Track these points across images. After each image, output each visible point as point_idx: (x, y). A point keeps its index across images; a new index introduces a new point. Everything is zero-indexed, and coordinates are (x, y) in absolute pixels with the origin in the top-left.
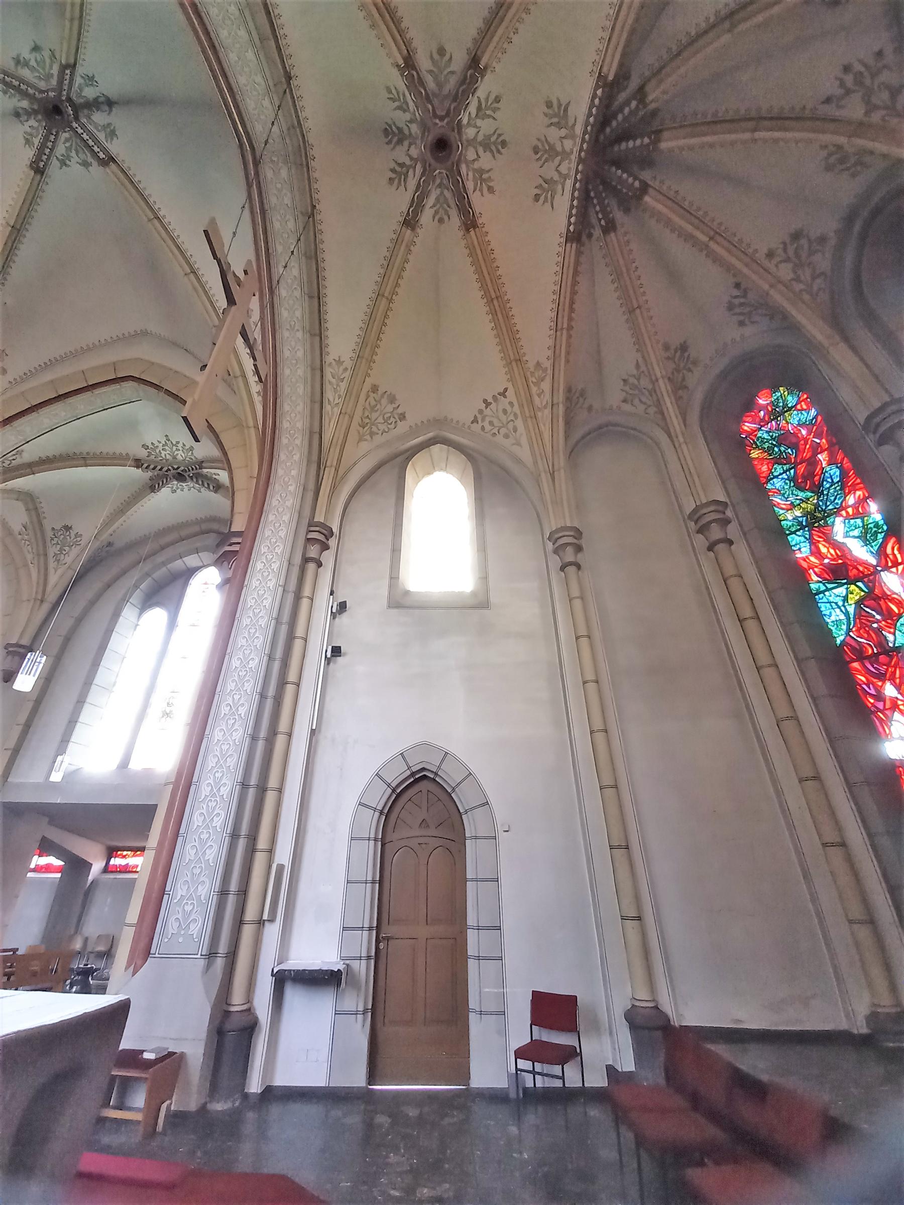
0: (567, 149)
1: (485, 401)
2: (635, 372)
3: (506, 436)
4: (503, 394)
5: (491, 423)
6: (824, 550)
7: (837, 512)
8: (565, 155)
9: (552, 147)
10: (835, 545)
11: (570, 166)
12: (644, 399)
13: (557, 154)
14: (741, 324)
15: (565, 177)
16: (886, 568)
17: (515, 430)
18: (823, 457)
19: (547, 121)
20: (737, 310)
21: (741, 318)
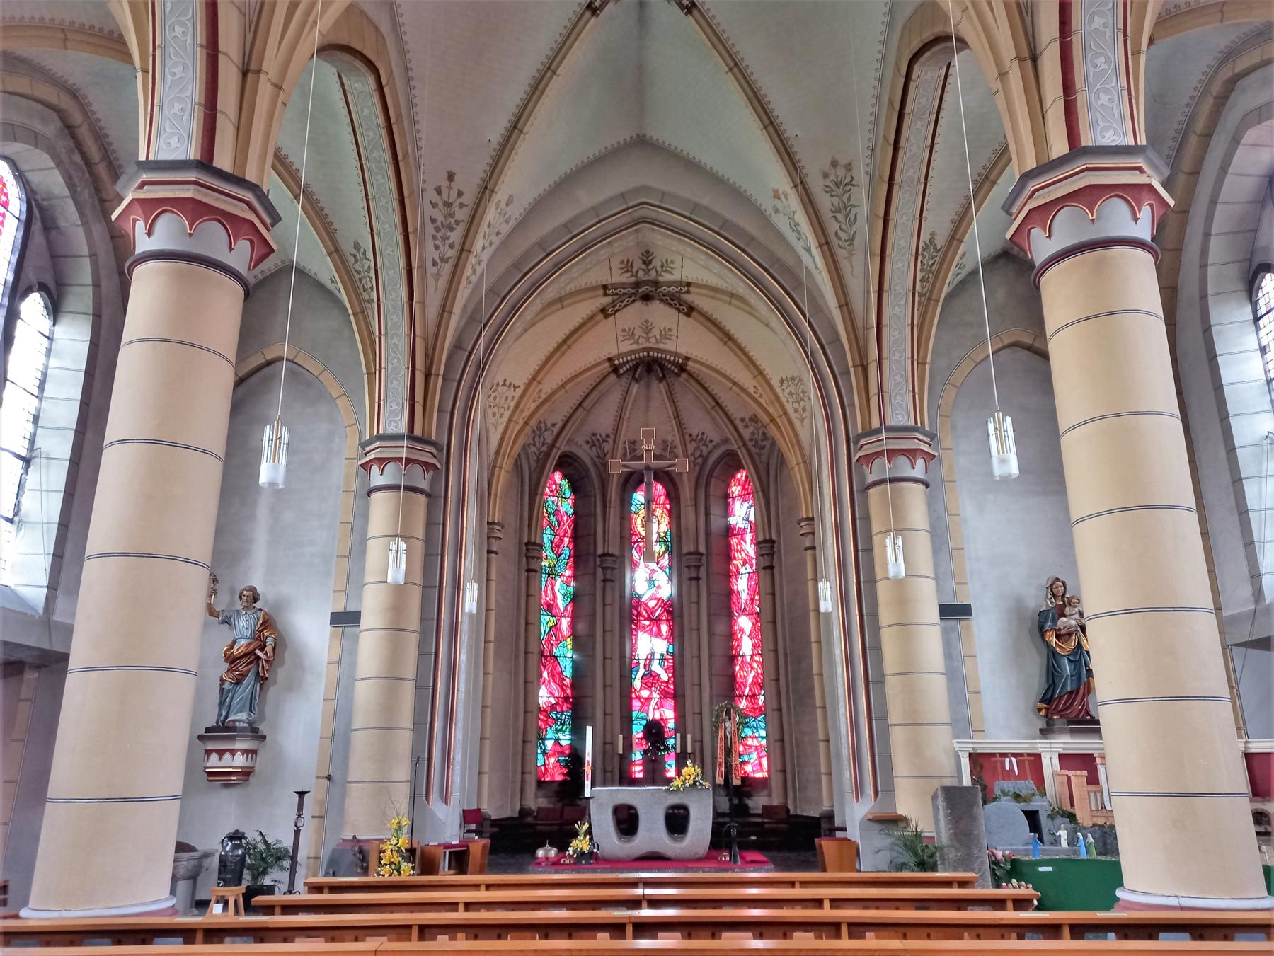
0: (651, 340)
1: (505, 380)
3: (494, 415)
4: (515, 387)
5: (495, 398)
6: (549, 592)
7: (560, 576)
8: (648, 339)
10: (554, 593)
12: (537, 438)
13: (647, 334)
14: (587, 442)
15: (637, 342)
16: (565, 616)
18: (566, 540)
19: (662, 329)
20: (594, 438)
21: (590, 440)
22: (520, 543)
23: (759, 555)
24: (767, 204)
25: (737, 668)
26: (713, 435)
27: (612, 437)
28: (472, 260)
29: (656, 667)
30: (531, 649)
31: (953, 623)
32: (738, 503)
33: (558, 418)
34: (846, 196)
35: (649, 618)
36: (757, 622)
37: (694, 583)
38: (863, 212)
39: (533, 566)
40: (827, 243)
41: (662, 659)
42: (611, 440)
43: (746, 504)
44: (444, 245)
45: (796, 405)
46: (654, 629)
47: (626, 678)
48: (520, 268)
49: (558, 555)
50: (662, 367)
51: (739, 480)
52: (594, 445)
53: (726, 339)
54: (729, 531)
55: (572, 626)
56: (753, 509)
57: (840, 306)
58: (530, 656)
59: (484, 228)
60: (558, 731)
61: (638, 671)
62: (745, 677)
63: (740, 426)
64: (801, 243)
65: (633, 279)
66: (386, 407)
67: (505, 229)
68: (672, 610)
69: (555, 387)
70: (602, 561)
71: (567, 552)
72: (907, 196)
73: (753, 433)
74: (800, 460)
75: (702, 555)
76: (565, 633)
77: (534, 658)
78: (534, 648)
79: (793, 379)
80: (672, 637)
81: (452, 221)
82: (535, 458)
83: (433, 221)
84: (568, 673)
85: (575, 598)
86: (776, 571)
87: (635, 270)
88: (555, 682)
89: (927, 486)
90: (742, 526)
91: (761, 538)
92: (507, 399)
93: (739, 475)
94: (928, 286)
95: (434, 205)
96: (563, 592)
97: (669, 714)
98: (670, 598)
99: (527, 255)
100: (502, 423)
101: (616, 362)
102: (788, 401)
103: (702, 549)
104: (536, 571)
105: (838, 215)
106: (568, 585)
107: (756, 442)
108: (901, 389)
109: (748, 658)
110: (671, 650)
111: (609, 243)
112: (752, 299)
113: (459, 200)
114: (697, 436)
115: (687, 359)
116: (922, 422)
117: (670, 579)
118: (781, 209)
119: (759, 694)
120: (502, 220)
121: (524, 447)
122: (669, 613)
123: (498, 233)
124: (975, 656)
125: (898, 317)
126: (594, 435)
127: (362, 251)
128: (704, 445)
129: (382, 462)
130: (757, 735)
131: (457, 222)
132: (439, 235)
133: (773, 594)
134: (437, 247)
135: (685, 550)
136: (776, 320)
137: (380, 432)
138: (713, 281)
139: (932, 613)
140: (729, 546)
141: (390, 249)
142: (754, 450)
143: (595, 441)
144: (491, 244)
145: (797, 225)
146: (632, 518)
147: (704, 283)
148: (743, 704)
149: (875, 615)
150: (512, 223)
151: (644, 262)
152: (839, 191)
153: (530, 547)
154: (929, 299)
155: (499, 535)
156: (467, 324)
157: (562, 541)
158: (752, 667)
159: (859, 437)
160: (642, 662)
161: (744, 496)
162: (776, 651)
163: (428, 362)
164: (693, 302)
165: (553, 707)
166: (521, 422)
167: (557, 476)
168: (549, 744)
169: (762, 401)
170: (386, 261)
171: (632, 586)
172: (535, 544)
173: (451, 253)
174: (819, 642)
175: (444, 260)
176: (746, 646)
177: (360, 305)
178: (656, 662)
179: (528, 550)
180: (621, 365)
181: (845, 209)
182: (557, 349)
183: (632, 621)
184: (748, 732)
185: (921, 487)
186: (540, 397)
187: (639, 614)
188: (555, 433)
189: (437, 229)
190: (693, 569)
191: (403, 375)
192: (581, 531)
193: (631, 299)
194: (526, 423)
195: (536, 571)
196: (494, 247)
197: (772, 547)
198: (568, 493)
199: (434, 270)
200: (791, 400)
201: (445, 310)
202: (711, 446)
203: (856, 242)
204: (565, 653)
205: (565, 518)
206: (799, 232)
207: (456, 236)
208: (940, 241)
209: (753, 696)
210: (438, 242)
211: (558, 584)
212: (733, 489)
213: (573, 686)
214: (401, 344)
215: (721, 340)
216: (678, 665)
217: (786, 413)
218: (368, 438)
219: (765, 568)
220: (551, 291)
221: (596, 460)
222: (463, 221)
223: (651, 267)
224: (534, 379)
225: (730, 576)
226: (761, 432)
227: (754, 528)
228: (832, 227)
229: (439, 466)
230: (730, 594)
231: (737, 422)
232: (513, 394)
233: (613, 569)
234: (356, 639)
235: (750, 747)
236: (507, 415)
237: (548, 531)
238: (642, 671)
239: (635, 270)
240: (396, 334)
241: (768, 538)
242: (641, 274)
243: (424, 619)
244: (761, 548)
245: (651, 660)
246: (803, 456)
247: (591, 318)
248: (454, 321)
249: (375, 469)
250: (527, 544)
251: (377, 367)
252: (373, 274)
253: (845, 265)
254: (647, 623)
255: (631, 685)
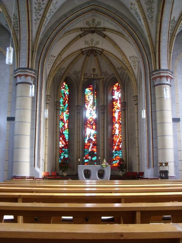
1: (52, 55)
2: (63, 68)
3: (48, 64)
4: (55, 57)
8: (92, 44)
9: (93, 42)
11: (91, 45)
12: (59, 72)
14: (73, 74)
15: (89, 45)
17: (50, 65)
18: (67, 101)
22: (54, 101)
23: (122, 106)
24: (129, 6)
25: (114, 138)
26: (110, 73)
27: (80, 72)
28: (46, 19)
29: (92, 137)
30: (57, 131)
31: (176, 123)
32: (116, 92)
33: (65, 65)
34: (151, 5)
35: (90, 124)
36: (120, 125)
37: (103, 114)
38: (155, 10)
39: (58, 108)
40: (145, 18)
41: (93, 135)
42: (80, 73)
43: (118, 92)
44: (38, 15)
45: (134, 64)
46: (91, 127)
47: (84, 141)
48: (59, 21)
49: (65, 106)
50: (95, 52)
51: (116, 86)
52: (75, 75)
53: (115, 45)
54: (113, 100)
55: (68, 126)
56: (120, 94)
57: (149, 36)
58: (57, 133)
59: (49, 11)
60: (65, 154)
61: (86, 138)
62: (116, 140)
63: (117, 70)
64: (138, 18)
65: (89, 27)
66: (21, 60)
67: (55, 11)
68: (96, 122)
69: (65, 57)
70: (77, 108)
71: (67, 105)
72: (168, 6)
73: (121, 72)
74: (135, 80)
75: (105, 106)
76: (66, 128)
77: (58, 134)
78: (58, 131)
79: (133, 57)
80: (96, 129)
81: (41, 8)
82: (59, 78)
83: (35, 8)
84: (67, 138)
85: (69, 118)
86: (126, 111)
87: (90, 24)
88: (63, 141)
89: (171, 86)
90: (117, 98)
91: (122, 102)
92: (52, 60)
93: (116, 84)
94: (172, 31)
95: (36, 4)
96: (66, 116)
97: (95, 150)
98: (96, 119)
99: (61, 18)
100: (50, 67)
101: (83, 50)
102: (131, 63)
103: (105, 104)
104: (59, 110)
105: (149, 11)
106: (67, 114)
107: (122, 74)
108: (165, 59)
109: (117, 135)
110: (96, 133)
111: (84, 16)
112: (124, 33)
113: (42, 2)
114: (105, 72)
115: (103, 50)
116: (170, 69)
117: (96, 113)
118: (133, 8)
119: (120, 145)
120: (54, 8)
121: (56, 75)
122: (96, 123)
123: (53, 12)
124: (180, 132)
125: (164, 39)
126: (75, 71)
127: (15, 16)
128: (107, 75)
129: (20, 75)
130: (119, 155)
131: (42, 9)
132: (37, 12)
133: (125, 117)
134: (36, 15)
135: (100, 105)
136: (131, 39)
137: (20, 67)
138: (112, 27)
139: (171, 121)
140: (113, 104)
141: (24, 16)
142: (121, 77)
143: (76, 73)
144: (51, 15)
145: (137, 13)
146: (85, 96)
147: (110, 28)
148: (116, 147)
149: (156, 120)
150: (57, 9)
151: (93, 22)
152: (149, 4)
153: (57, 103)
154: (173, 35)
155: (49, 99)
156: (43, 38)
157: (65, 102)
158: (118, 137)
159: (153, 72)
160: (88, 136)
161: (118, 90)
162: (125, 133)
163: (33, 48)
164: (106, 34)
165: (63, 148)
166: (56, 67)
167: (64, 84)
168: (62, 157)
169: (124, 63)
170: (22, 19)
171: (85, 115)
172: (58, 102)
173: (40, 17)
174: (138, 130)
175: (38, 19)
176: (117, 132)
177: (15, 32)
178: (92, 136)
179: (56, 104)
180: (84, 51)
181: (150, 9)
182: (66, 46)
183: (85, 125)
184: (117, 155)
185: (169, 86)
186: (61, 60)
187: (87, 123)
188: (64, 71)
189: (36, 10)
190: (103, 110)
191: (26, 51)
192: (71, 99)
193: (88, 32)
194: (57, 67)
195: (59, 110)
196: (51, 16)
197: (125, 104)
198: (67, 88)
199: (35, 22)
200: (132, 63)
201: (38, 33)
202: (109, 75)
203: (153, 18)
204: (66, 133)
205: (66, 95)
206: (137, 15)
207: (41, 12)
208: (176, 19)
209: (118, 145)
210: (36, 14)
211: (65, 114)
212: (114, 88)
213: (68, 142)
214: (26, 42)
215: (113, 45)
216: (97, 137)
217: (131, 66)
218: (16, 69)
219: (123, 110)
220: (67, 29)
221: (76, 79)
222: (43, 8)
223: (94, 23)
224: (59, 54)
225: (113, 113)
226: (123, 72)
227: (120, 99)
228: (147, 14)
229: (36, 77)
230: (114, 117)
231: (117, 69)
232: (54, 59)
233: (80, 110)
234: (14, 125)
235: (117, 158)
236: (52, 64)
237: (62, 99)
238: (88, 138)
239: (90, 24)
240: (25, 40)
241: (124, 101)
242: (91, 25)
243: (32, 120)
244: (122, 105)
245: (90, 135)
246: (135, 79)
247: (77, 37)
248: (40, 36)
249: (18, 78)
250: (56, 102)
251: (19, 49)
252: (18, 23)
253: (150, 24)
254: (89, 125)
255: (85, 142)
